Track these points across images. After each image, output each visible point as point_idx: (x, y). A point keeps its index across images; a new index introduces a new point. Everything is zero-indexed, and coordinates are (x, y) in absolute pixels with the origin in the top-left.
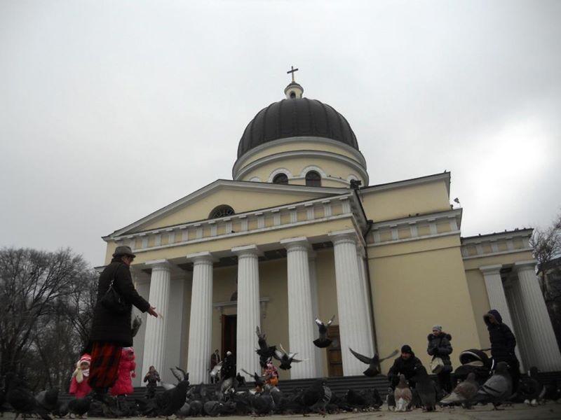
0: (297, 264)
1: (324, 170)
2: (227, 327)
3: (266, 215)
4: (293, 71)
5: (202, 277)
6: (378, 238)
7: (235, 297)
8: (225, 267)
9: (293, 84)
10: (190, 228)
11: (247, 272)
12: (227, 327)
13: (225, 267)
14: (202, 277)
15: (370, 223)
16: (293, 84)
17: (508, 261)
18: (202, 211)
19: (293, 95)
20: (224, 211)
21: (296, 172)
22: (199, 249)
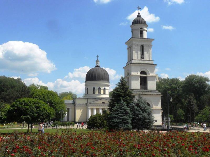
4: (98, 56)
9: (97, 61)
18: (101, 102)
20: (103, 103)
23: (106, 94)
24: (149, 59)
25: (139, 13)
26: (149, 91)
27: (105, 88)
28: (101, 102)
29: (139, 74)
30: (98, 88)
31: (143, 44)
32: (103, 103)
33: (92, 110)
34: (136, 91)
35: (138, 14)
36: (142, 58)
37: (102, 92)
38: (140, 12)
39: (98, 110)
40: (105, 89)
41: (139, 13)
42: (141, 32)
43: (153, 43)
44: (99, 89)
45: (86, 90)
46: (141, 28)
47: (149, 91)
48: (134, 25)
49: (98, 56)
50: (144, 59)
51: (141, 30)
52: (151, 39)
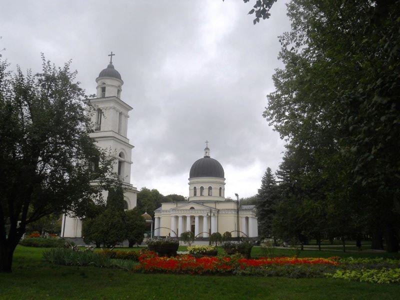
0: (205, 219)
1: (213, 186)
2: (193, 227)
3: (200, 210)
5: (188, 220)
6: (220, 212)
7: (194, 222)
8: (193, 218)
9: (207, 149)
10: (186, 210)
11: (197, 220)
12: (193, 227)
13: (193, 218)
14: (188, 220)
15: (219, 210)
16: (207, 149)
17: (247, 216)
19: (206, 152)
20: (192, 208)
21: (206, 187)
22: (188, 215)
23: (213, 195)
25: (111, 63)
27: (195, 188)
28: (188, 207)
30: (199, 188)
32: (192, 208)
33: (177, 217)
35: (109, 63)
37: (206, 192)
38: (112, 61)
39: (185, 218)
40: (210, 188)
41: (111, 63)
42: (104, 90)
44: (202, 188)
45: (190, 190)
51: (104, 86)
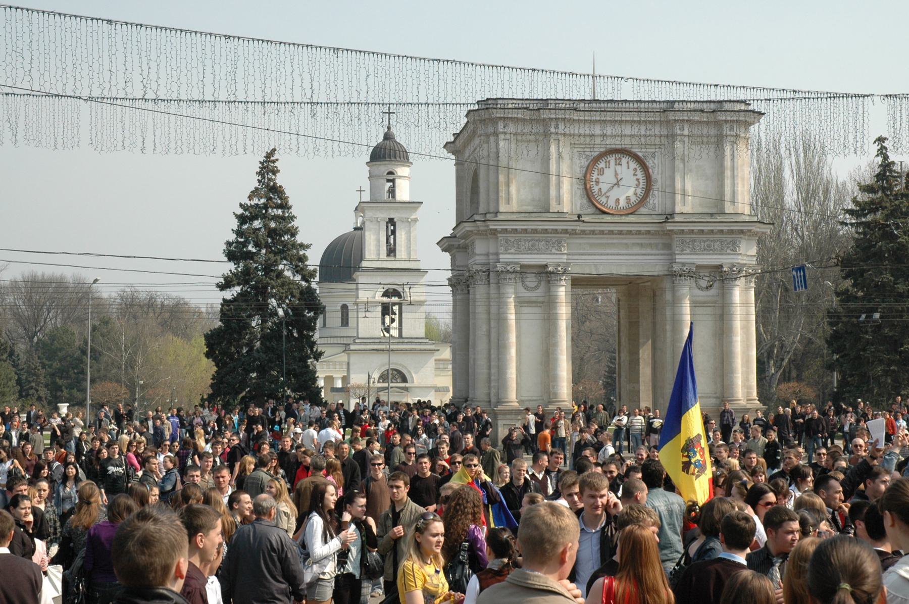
4: (361, 191)
24: (409, 254)
25: (389, 128)
26: (406, 341)
29: (379, 297)
31: (392, 217)
34: (371, 341)
36: (391, 251)
41: (389, 128)
43: (419, 214)
46: (391, 173)
47: (406, 341)
48: (374, 163)
49: (361, 191)
50: (395, 256)
51: (391, 177)
52: (414, 203)
